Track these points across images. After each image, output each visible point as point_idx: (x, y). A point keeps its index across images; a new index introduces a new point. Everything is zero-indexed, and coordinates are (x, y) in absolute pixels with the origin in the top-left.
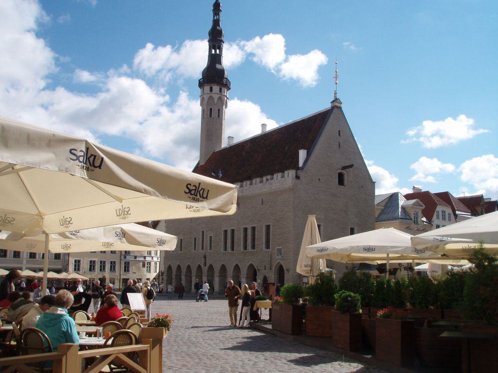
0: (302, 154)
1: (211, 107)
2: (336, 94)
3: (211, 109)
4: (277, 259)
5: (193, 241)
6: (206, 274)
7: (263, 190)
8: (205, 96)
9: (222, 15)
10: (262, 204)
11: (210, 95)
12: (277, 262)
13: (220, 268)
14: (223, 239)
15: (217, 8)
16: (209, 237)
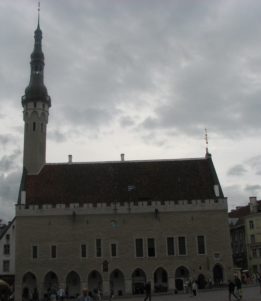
0: (216, 188)
1: (42, 122)
2: (207, 149)
3: (42, 124)
4: (216, 260)
5: (81, 249)
6: (109, 279)
7: (195, 210)
8: (37, 110)
9: (44, 42)
10: (192, 220)
11: (43, 111)
12: (216, 263)
13: (133, 272)
14: (135, 246)
15: (38, 35)
16: (111, 245)
